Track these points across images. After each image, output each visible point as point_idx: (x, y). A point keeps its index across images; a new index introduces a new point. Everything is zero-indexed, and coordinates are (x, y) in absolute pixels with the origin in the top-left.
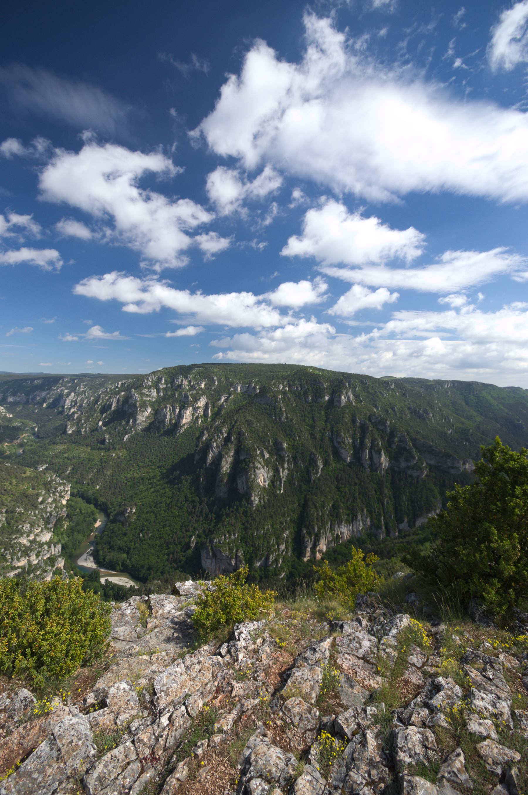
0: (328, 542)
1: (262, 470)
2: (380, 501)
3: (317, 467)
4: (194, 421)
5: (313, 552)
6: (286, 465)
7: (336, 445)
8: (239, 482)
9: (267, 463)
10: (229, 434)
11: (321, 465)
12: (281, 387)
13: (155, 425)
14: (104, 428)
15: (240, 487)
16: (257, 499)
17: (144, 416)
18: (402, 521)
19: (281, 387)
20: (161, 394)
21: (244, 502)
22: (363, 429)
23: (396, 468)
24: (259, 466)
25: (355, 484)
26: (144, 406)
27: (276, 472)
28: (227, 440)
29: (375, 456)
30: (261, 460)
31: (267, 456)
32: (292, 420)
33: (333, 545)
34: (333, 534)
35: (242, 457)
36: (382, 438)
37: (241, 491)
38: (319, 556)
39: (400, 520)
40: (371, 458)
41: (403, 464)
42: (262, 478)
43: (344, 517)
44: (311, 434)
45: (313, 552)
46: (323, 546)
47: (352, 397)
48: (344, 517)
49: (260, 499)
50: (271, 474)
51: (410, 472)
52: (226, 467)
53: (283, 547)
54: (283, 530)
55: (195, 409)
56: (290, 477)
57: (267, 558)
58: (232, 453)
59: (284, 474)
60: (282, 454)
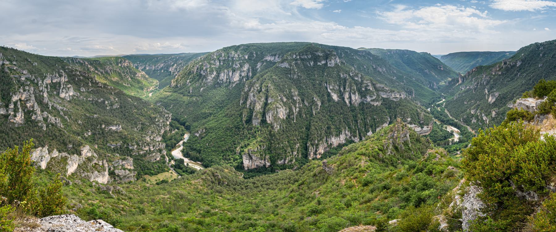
0: (325, 148)
1: (282, 109)
2: (356, 121)
3: (317, 105)
4: (241, 80)
5: (315, 154)
6: (297, 105)
7: (329, 90)
8: (267, 117)
9: (285, 104)
10: (261, 88)
11: (319, 104)
12: (294, 56)
13: (217, 84)
14: (190, 84)
15: (268, 119)
16: (278, 126)
17: (210, 78)
18: (369, 131)
19: (294, 56)
20: (222, 64)
21: (270, 128)
22: (345, 80)
23: (365, 102)
24: (280, 106)
25: (341, 114)
26: (211, 72)
27: (291, 109)
28: (260, 91)
29: (353, 96)
30: (281, 103)
31: (285, 100)
32: (301, 77)
33: (328, 149)
34: (328, 144)
35: (269, 102)
36: (357, 85)
37: (269, 122)
38: (318, 156)
39: (367, 131)
40: (350, 97)
41: (369, 99)
42: (282, 114)
43: (334, 133)
44: (314, 85)
45: (315, 154)
46: (321, 150)
47: (338, 61)
48: (334, 133)
49: (280, 126)
50: (288, 111)
51: (372, 103)
52: (258, 107)
53: (295, 153)
54: (295, 144)
55: (241, 72)
56: (300, 113)
57: (285, 160)
58: (263, 99)
59: (296, 111)
60: (295, 98)
